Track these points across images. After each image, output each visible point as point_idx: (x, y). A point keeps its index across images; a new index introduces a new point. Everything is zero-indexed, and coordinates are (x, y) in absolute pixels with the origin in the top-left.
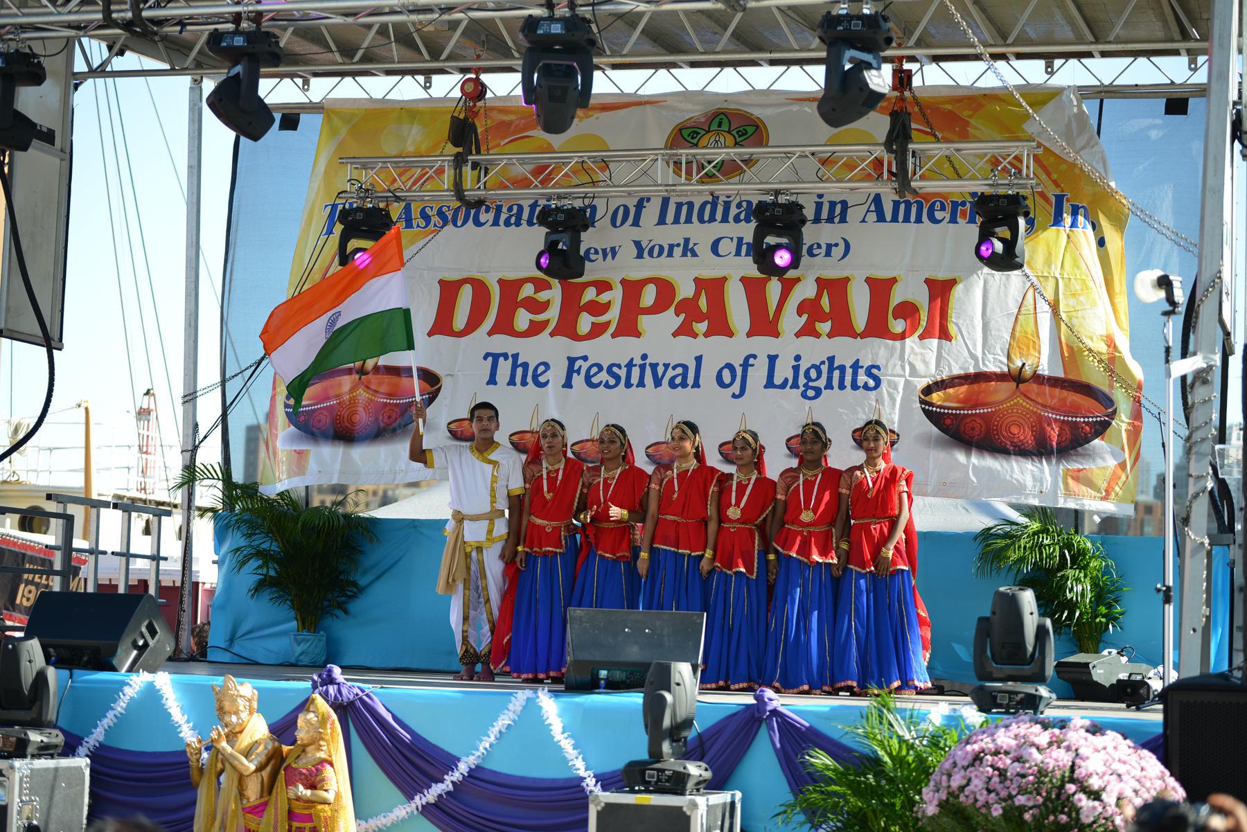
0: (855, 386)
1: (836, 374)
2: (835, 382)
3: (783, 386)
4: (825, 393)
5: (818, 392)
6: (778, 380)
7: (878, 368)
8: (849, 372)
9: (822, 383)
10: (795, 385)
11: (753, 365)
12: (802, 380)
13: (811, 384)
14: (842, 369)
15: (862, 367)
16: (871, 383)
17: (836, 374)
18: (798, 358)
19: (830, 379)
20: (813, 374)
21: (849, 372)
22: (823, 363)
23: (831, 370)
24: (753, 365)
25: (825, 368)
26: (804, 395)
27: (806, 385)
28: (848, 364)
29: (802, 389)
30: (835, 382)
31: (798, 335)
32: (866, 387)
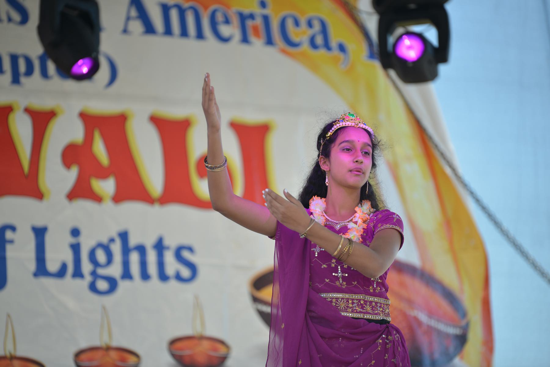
0: (163, 277)
1: (134, 257)
2: (135, 269)
3: (61, 273)
4: (123, 285)
5: (113, 284)
6: (52, 266)
7: (190, 249)
8: (152, 257)
9: (115, 270)
10: (78, 273)
11: (11, 242)
12: (87, 267)
13: (101, 271)
14: (141, 249)
15: (168, 248)
16: (186, 273)
17: (134, 257)
18: (75, 232)
19: (126, 264)
20: (101, 256)
21: (152, 257)
22: (112, 240)
23: (126, 251)
24: (11, 242)
25: (116, 248)
26: (93, 288)
27: (94, 274)
28: (149, 242)
29: (88, 278)
30: (135, 269)
31: (72, 196)
32: (179, 277)
